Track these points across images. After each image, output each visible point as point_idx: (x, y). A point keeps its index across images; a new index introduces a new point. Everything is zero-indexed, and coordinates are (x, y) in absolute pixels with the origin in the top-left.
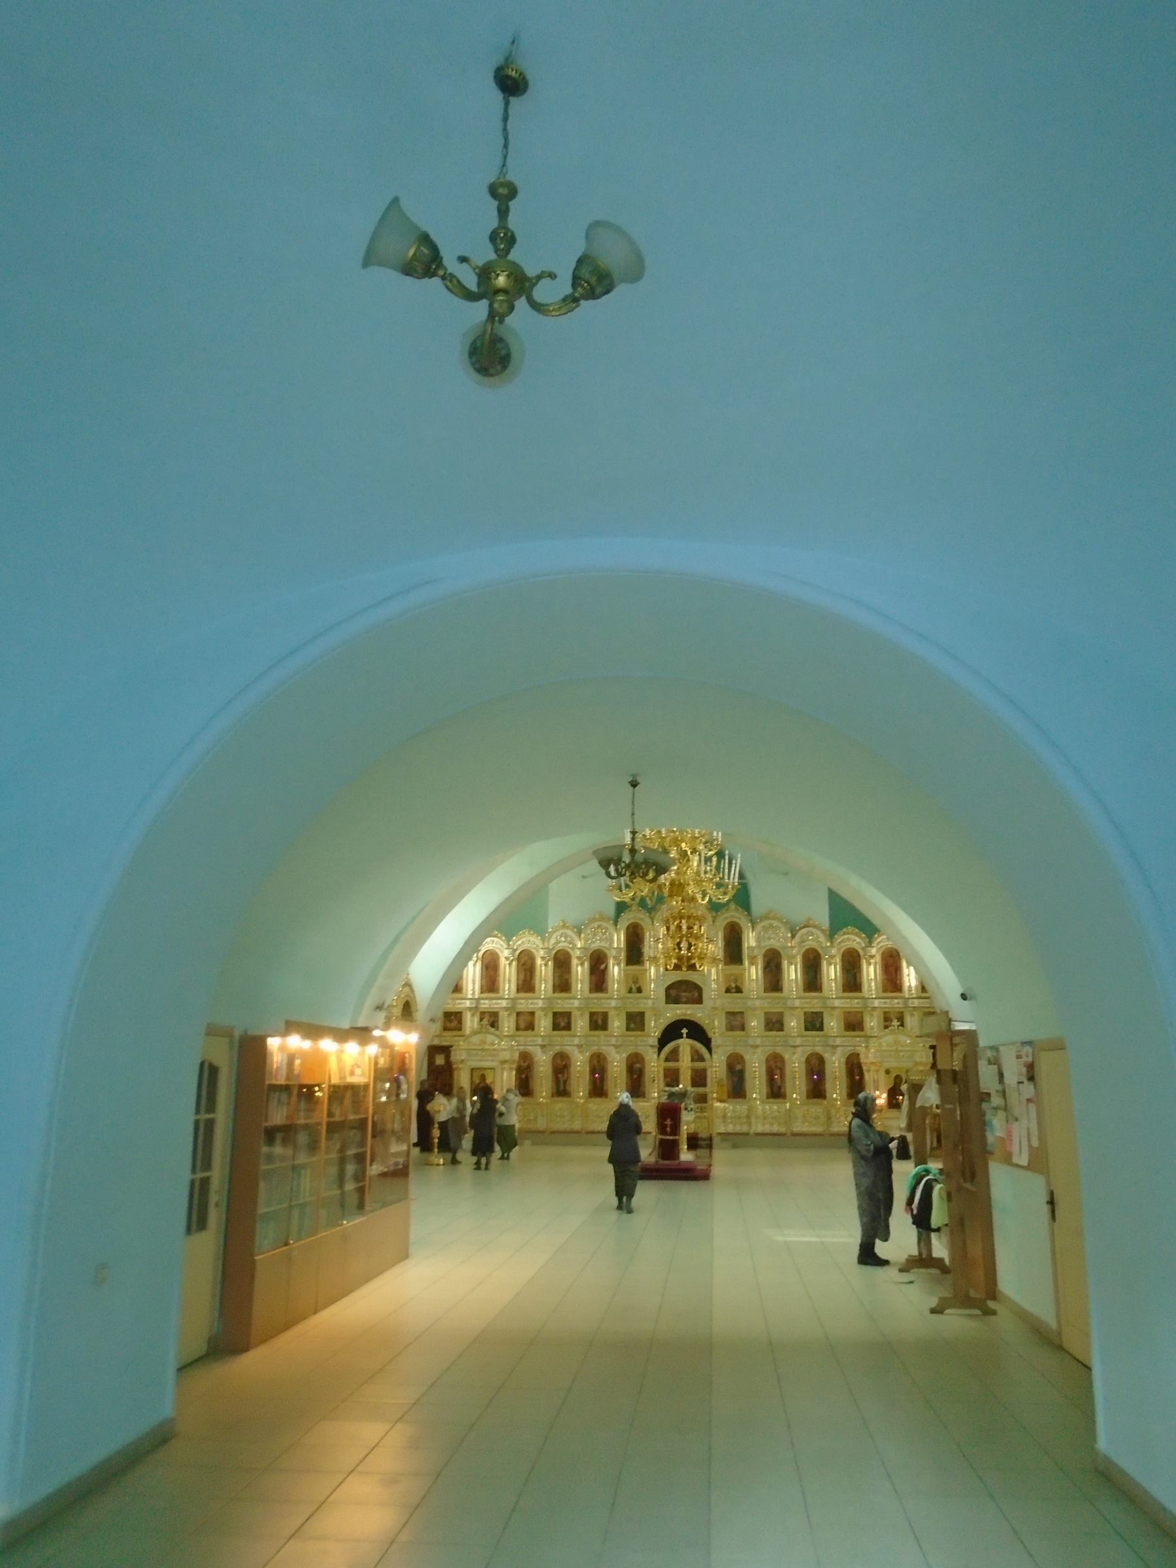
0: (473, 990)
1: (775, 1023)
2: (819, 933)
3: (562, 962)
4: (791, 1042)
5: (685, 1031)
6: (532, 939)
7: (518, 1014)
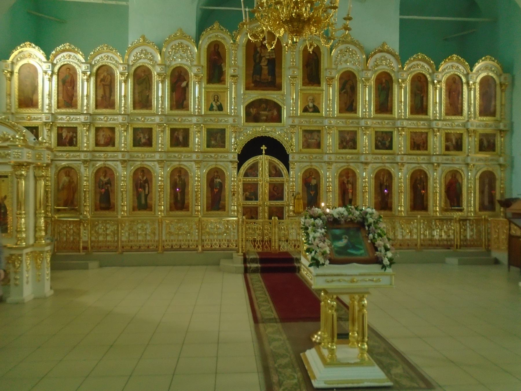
0: (50, 105)
1: (348, 141)
2: (392, 59)
3: (142, 79)
4: (363, 159)
5: (264, 148)
6: (110, 55)
7: (98, 129)
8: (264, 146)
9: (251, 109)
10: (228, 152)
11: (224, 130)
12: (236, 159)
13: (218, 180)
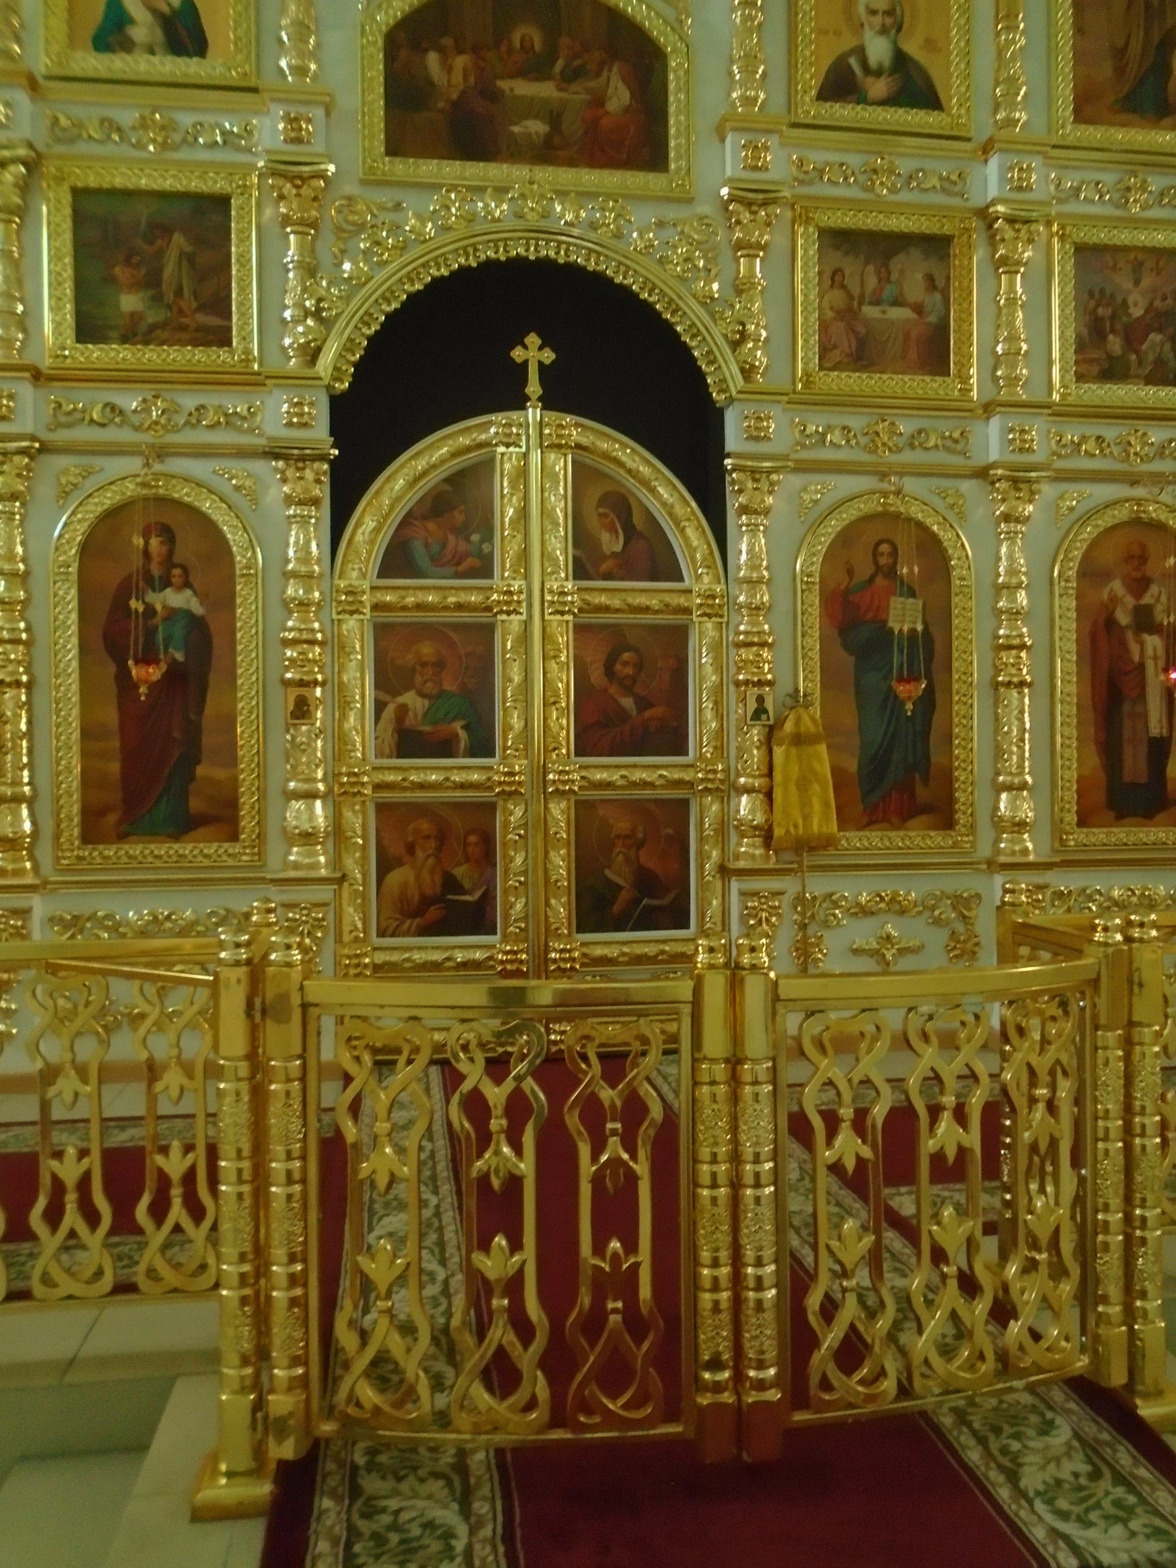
8: (533, 340)
9: (433, 59)
10: (250, 381)
11: (222, 202)
12: (320, 433)
13: (176, 599)
